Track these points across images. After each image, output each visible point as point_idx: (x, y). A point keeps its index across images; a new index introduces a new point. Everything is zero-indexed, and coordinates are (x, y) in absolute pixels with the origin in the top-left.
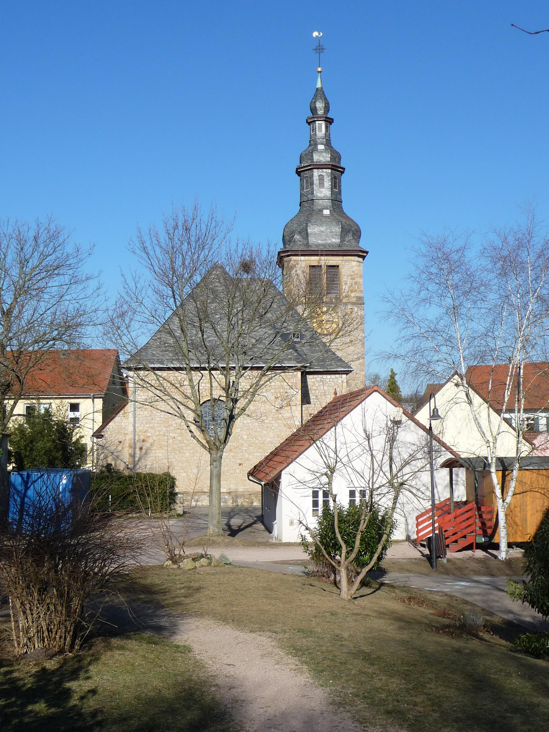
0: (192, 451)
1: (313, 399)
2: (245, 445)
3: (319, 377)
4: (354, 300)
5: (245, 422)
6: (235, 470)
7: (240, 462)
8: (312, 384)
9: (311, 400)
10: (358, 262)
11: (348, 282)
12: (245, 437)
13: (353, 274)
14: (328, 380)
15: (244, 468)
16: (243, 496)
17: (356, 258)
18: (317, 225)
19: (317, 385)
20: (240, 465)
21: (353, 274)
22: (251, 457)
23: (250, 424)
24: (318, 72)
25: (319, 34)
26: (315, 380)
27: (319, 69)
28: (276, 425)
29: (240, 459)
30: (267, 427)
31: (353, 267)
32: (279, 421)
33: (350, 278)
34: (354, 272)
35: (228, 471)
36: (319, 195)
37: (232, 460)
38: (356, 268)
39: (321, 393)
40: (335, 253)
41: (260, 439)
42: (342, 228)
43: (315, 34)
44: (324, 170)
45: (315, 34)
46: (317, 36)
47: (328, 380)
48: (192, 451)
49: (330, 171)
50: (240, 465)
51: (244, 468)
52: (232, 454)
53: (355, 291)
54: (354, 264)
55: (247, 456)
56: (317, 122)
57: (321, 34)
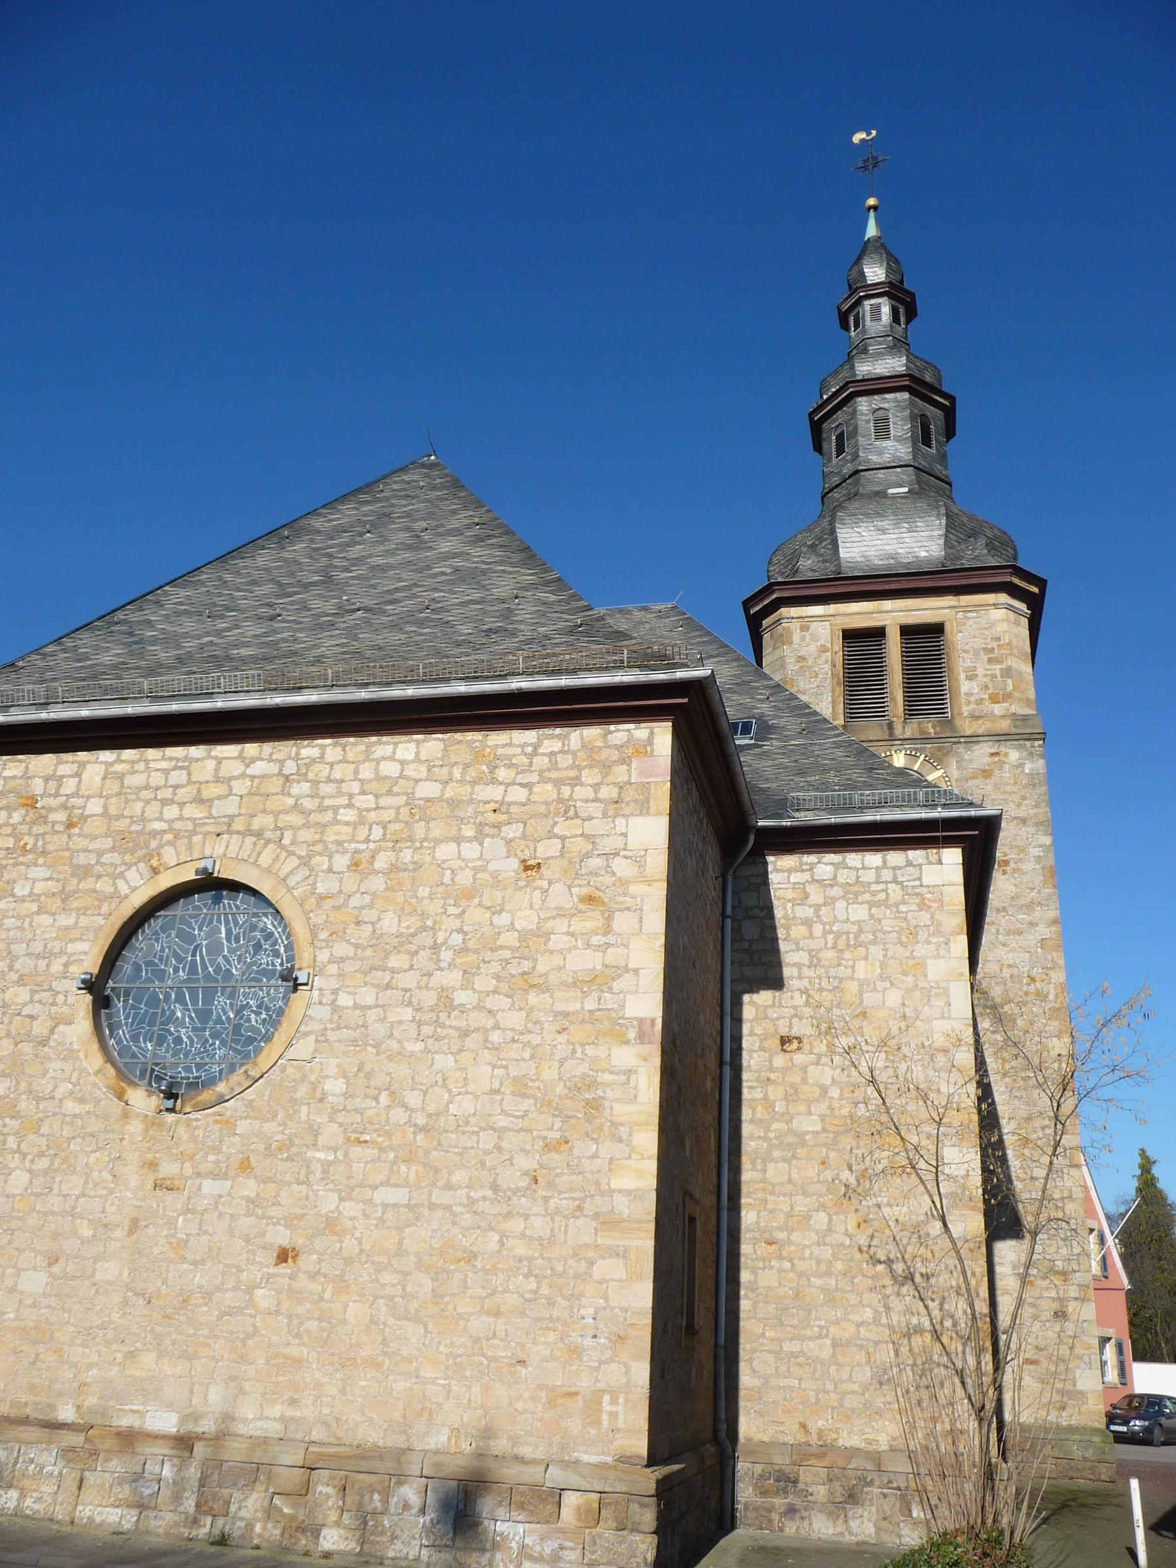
0: (43, 1164)
1: (799, 966)
2: (331, 1133)
3: (825, 864)
4: (1005, 725)
5: (344, 1000)
6: (250, 1290)
7: (282, 1237)
8: (790, 895)
9: (787, 972)
10: (1010, 608)
11: (980, 672)
12: (335, 1086)
13: (995, 644)
14: (870, 876)
15: (302, 1282)
16: (255, 1472)
17: (1003, 598)
18: (867, 515)
19: (816, 896)
20: (283, 1256)
21: (995, 644)
22: (351, 1209)
23: (372, 1015)
24: (869, 208)
25: (869, 134)
26: (806, 876)
27: (872, 201)
28: (514, 1020)
29: (290, 1222)
30: (464, 1033)
31: (992, 625)
32: (533, 998)
33: (985, 658)
34: (999, 639)
35: (207, 1295)
36: (874, 458)
37: (246, 1224)
38: (1004, 626)
39: (838, 935)
40: (929, 584)
41: (414, 1099)
42: (947, 515)
43: (858, 137)
44: (888, 396)
45: (858, 137)
46: (862, 141)
47: (870, 876)
48: (43, 1164)
49: (906, 395)
50: (283, 1256)
51: (302, 1282)
52: (249, 1187)
53: (1007, 697)
54: (1000, 614)
55: (329, 1203)
56: (867, 304)
57: (874, 133)
